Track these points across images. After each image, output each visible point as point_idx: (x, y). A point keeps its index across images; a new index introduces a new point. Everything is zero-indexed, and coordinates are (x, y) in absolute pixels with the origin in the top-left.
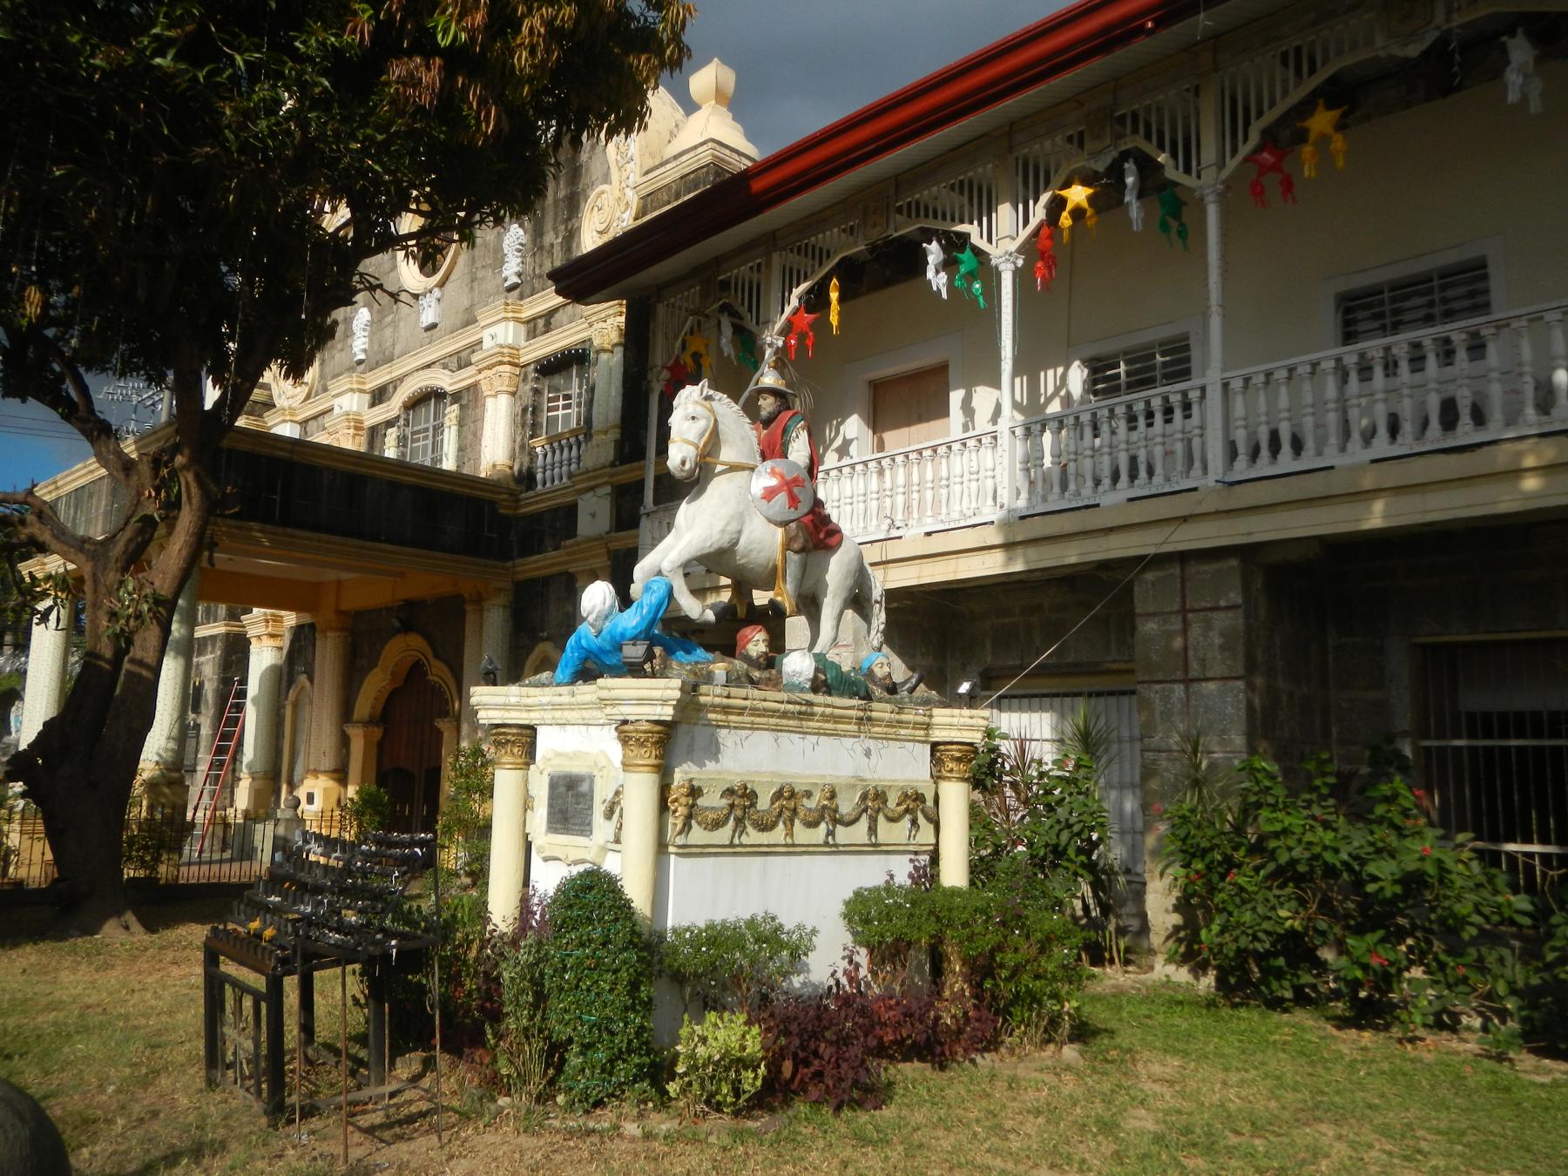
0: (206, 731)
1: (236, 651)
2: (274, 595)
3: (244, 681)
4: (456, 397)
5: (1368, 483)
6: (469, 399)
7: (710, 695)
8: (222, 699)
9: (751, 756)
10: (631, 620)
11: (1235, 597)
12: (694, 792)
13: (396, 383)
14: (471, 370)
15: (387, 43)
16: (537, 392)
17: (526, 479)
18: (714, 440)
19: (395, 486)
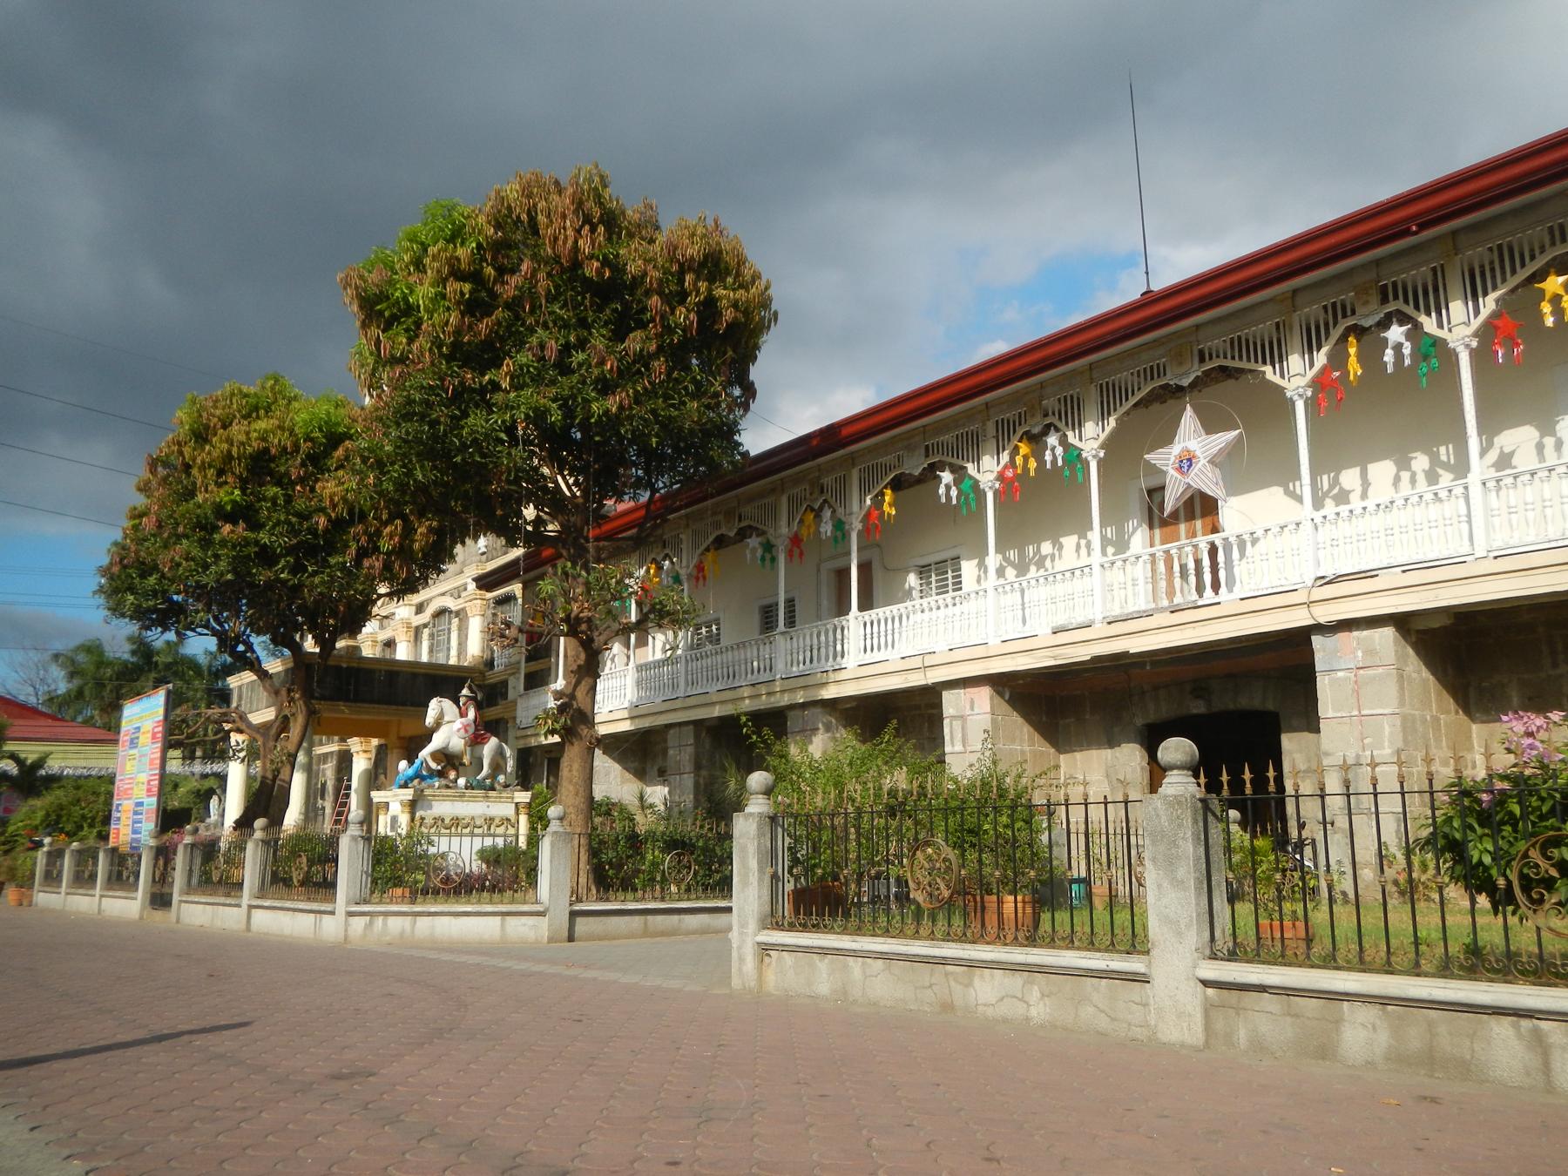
0: (328, 811)
1: (345, 760)
2: (365, 732)
3: (350, 780)
4: (458, 614)
5: (715, 699)
6: (461, 614)
7: (427, 792)
8: (337, 790)
9: (444, 808)
10: (411, 772)
11: (691, 741)
12: (422, 819)
13: (429, 601)
14: (461, 601)
15: (362, 553)
16: (494, 615)
17: (490, 664)
18: (441, 715)
19: (414, 675)
